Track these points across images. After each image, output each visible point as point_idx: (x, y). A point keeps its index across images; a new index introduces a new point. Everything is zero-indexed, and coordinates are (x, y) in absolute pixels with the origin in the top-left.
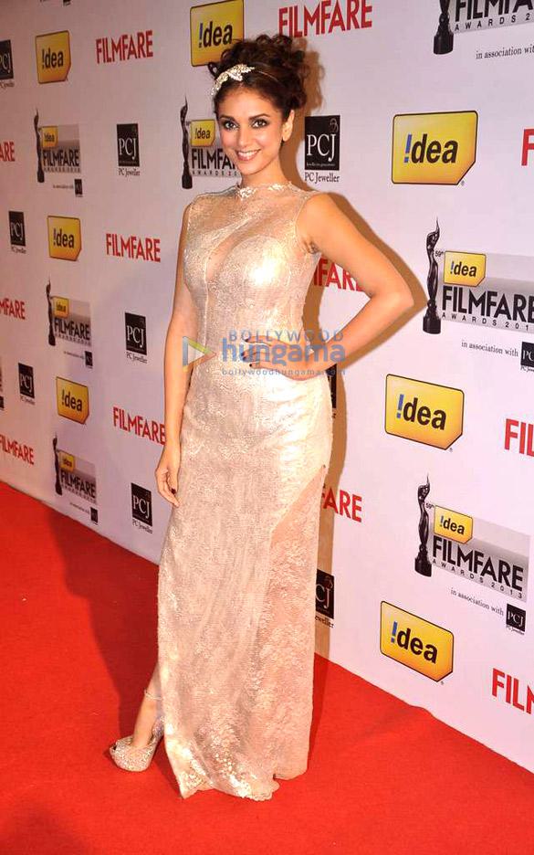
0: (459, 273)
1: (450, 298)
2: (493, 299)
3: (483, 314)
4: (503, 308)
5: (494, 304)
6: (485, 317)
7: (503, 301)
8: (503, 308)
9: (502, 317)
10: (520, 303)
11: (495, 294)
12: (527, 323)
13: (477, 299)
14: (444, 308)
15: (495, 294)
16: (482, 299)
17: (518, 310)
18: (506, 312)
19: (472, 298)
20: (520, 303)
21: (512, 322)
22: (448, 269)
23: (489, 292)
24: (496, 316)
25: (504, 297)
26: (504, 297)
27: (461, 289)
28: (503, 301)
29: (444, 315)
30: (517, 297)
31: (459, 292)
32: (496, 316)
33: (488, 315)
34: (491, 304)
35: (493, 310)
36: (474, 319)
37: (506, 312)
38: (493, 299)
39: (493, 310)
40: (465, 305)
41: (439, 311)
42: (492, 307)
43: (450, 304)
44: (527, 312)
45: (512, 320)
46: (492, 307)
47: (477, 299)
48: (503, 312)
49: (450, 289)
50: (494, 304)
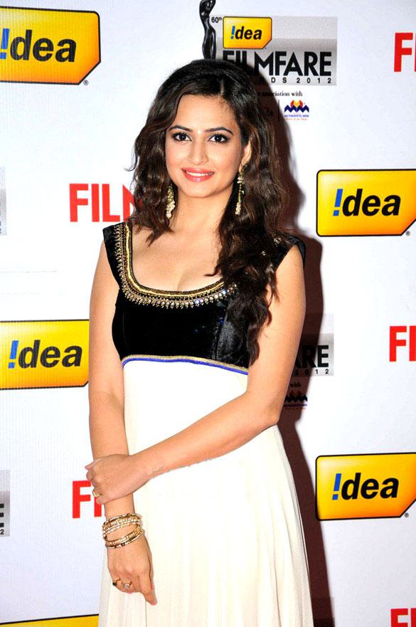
0: (241, 37)
2: (282, 58)
3: (271, 73)
4: (293, 66)
5: (284, 63)
6: (274, 76)
7: (293, 59)
8: (293, 66)
9: (293, 75)
10: (311, 59)
11: (284, 54)
12: (319, 77)
13: (264, 59)
15: (284, 54)
16: (270, 60)
17: (307, 65)
18: (297, 69)
20: (311, 59)
21: (304, 78)
22: (228, 33)
23: (277, 53)
24: (286, 73)
25: (293, 55)
26: (293, 55)
28: (293, 59)
30: (307, 55)
32: (286, 73)
33: (277, 73)
34: (279, 63)
35: (283, 69)
37: (297, 69)
38: (282, 58)
39: (283, 69)
42: (281, 66)
44: (319, 67)
45: (304, 76)
46: (281, 66)
47: (264, 59)
48: (293, 70)
49: (232, 53)
50: (284, 63)
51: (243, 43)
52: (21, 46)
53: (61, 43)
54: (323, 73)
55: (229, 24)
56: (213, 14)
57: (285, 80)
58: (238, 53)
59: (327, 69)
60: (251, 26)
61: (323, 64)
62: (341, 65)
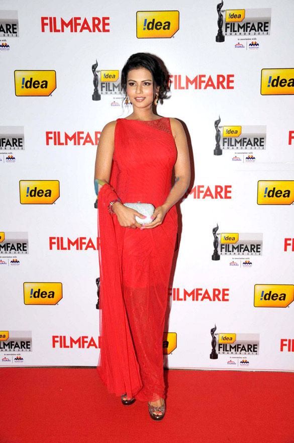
1: (229, 27)
9: (253, 32)
11: (249, 23)
14: (226, 31)
15: (249, 23)
16: (244, 26)
19: (239, 26)
22: (228, 16)
27: (234, 24)
29: (226, 34)
31: (233, 25)
32: (250, 31)
36: (240, 34)
37: (255, 29)
38: (248, 25)
39: (249, 29)
40: (236, 29)
41: (224, 33)
43: (229, 30)
47: (241, 26)
48: (253, 29)
49: (229, 24)
51: (234, 20)
52: (151, 25)
53: (165, 23)
54: (265, 30)
55: (228, 13)
56: (222, 9)
57: (249, 34)
58: (231, 24)
59: (266, 29)
60: (237, 13)
61: (265, 27)
62: (272, 27)
